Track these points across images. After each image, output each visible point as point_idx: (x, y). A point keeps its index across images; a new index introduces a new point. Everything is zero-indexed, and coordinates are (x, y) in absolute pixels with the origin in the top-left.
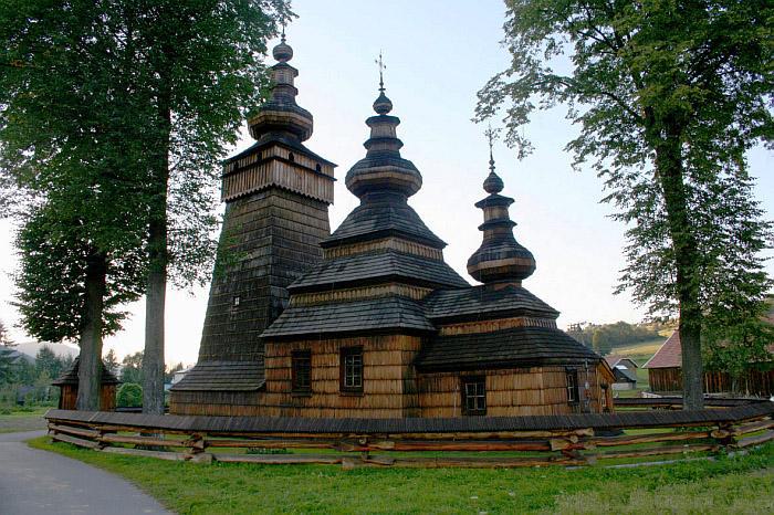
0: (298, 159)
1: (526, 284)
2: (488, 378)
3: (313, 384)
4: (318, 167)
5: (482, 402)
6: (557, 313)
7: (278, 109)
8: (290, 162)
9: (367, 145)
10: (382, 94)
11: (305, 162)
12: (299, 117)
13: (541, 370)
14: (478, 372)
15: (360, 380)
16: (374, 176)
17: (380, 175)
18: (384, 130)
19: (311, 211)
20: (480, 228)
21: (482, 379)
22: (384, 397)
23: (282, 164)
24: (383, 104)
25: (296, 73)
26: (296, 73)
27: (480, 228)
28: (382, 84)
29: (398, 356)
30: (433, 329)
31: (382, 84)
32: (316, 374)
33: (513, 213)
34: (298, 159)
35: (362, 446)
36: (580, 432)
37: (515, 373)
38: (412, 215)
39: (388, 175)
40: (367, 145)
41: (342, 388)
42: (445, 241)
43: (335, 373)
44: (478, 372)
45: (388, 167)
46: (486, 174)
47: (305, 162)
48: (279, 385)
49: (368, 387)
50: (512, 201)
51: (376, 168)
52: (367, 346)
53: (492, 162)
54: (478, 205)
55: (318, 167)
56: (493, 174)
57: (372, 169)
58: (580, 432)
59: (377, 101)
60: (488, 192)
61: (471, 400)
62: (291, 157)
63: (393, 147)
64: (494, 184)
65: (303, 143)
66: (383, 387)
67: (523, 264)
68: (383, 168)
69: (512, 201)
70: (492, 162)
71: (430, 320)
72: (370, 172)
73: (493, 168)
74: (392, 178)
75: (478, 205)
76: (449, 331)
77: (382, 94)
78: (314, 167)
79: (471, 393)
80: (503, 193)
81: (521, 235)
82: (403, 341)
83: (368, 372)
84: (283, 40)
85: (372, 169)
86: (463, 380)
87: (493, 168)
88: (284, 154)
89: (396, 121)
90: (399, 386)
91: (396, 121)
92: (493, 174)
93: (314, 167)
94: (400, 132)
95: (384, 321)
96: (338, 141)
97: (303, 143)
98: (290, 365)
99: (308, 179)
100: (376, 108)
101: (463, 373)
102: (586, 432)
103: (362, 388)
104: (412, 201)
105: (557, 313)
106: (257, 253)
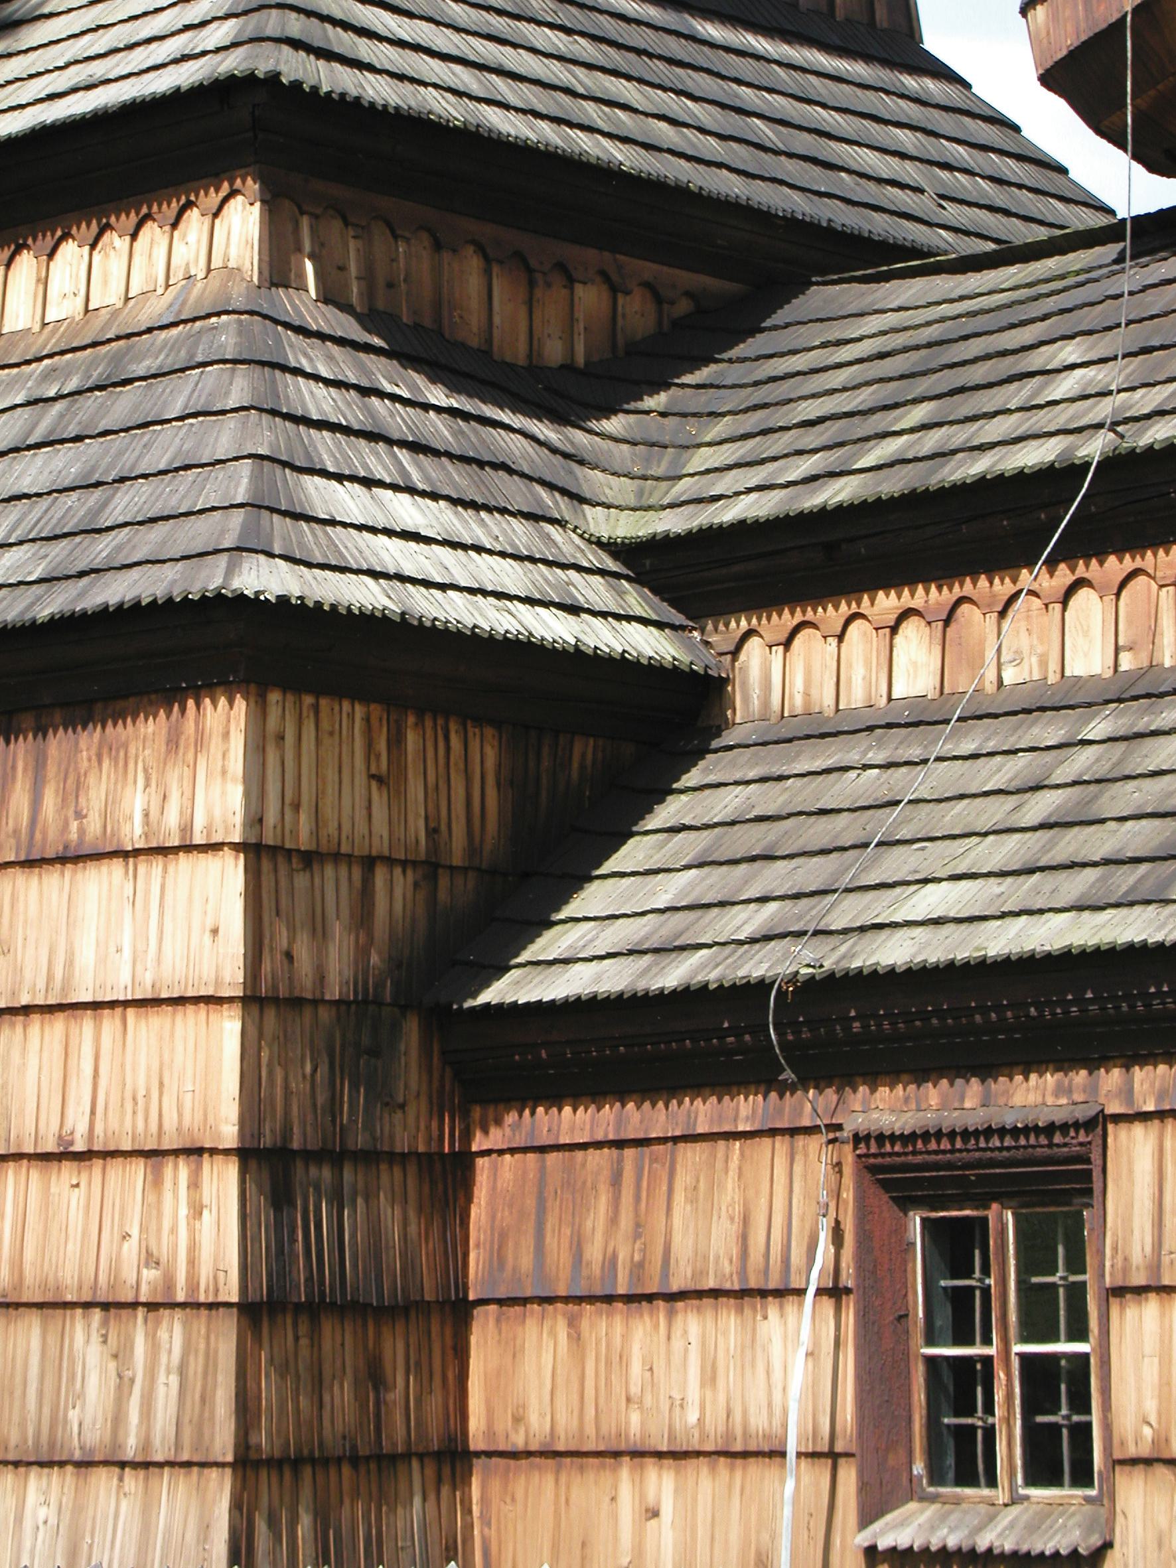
2: (1133, 1156)
5: (1061, 1391)
14: (1034, 1095)
21: (1057, 1182)
22: (85, 1338)
29: (201, 920)
30: (648, 644)
61: (962, 1385)
71: (642, 561)
76: (787, 667)
79: (961, 1315)
82: (199, 769)
86: (896, 1173)
90: (205, 1229)
95: (101, 549)
101: (886, 1108)
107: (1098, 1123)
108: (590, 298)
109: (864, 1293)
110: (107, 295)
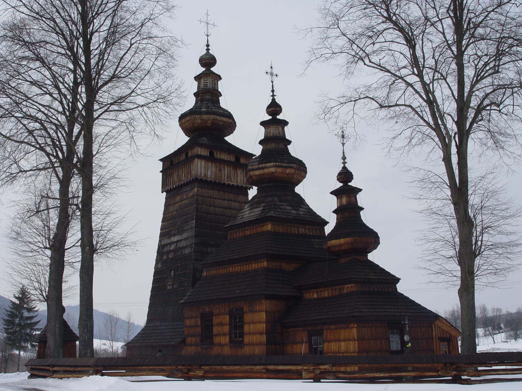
0: (219, 155)
1: (372, 256)
2: (325, 332)
3: (214, 338)
4: (237, 159)
6: (397, 280)
7: (201, 113)
8: (210, 158)
9: (261, 143)
10: (274, 100)
11: (224, 157)
12: (218, 118)
13: (355, 326)
14: (319, 328)
15: (242, 335)
16: (262, 172)
17: (266, 171)
18: (274, 130)
19: (232, 196)
20: (334, 212)
24: (274, 108)
25: (219, 78)
26: (219, 78)
27: (334, 212)
28: (273, 91)
31: (273, 91)
32: (215, 330)
33: (361, 199)
34: (219, 155)
35: (186, 373)
37: (340, 329)
38: (300, 201)
39: (273, 170)
40: (261, 143)
41: (231, 341)
42: (327, 220)
43: (226, 329)
44: (319, 328)
45: (272, 164)
46: (339, 168)
47: (224, 157)
48: (193, 339)
49: (247, 339)
50: (360, 190)
51: (263, 165)
52: (245, 309)
53: (344, 158)
54: (332, 193)
55: (237, 159)
56: (344, 168)
57: (260, 166)
58: (322, 367)
59: (268, 108)
62: (211, 154)
63: (281, 146)
64: (345, 176)
65: (227, 139)
66: (255, 338)
67: (372, 239)
68: (268, 165)
69: (360, 190)
70: (344, 158)
72: (258, 169)
73: (344, 163)
74: (276, 172)
75: (332, 193)
77: (274, 100)
78: (232, 159)
80: (352, 184)
81: (367, 218)
83: (246, 328)
84: (208, 50)
85: (260, 166)
87: (344, 163)
89: (285, 123)
90: (263, 338)
91: (285, 123)
92: (344, 168)
93: (232, 159)
94: (289, 132)
96: (247, 138)
97: (227, 139)
98: (199, 324)
99: (226, 170)
100: (269, 113)
101: (310, 328)
102: (326, 367)
103: (243, 340)
104: (298, 189)
105: (397, 280)
106: (185, 235)
107: (323, 330)
108: (294, 265)
109: (310, 342)
110: (256, 267)
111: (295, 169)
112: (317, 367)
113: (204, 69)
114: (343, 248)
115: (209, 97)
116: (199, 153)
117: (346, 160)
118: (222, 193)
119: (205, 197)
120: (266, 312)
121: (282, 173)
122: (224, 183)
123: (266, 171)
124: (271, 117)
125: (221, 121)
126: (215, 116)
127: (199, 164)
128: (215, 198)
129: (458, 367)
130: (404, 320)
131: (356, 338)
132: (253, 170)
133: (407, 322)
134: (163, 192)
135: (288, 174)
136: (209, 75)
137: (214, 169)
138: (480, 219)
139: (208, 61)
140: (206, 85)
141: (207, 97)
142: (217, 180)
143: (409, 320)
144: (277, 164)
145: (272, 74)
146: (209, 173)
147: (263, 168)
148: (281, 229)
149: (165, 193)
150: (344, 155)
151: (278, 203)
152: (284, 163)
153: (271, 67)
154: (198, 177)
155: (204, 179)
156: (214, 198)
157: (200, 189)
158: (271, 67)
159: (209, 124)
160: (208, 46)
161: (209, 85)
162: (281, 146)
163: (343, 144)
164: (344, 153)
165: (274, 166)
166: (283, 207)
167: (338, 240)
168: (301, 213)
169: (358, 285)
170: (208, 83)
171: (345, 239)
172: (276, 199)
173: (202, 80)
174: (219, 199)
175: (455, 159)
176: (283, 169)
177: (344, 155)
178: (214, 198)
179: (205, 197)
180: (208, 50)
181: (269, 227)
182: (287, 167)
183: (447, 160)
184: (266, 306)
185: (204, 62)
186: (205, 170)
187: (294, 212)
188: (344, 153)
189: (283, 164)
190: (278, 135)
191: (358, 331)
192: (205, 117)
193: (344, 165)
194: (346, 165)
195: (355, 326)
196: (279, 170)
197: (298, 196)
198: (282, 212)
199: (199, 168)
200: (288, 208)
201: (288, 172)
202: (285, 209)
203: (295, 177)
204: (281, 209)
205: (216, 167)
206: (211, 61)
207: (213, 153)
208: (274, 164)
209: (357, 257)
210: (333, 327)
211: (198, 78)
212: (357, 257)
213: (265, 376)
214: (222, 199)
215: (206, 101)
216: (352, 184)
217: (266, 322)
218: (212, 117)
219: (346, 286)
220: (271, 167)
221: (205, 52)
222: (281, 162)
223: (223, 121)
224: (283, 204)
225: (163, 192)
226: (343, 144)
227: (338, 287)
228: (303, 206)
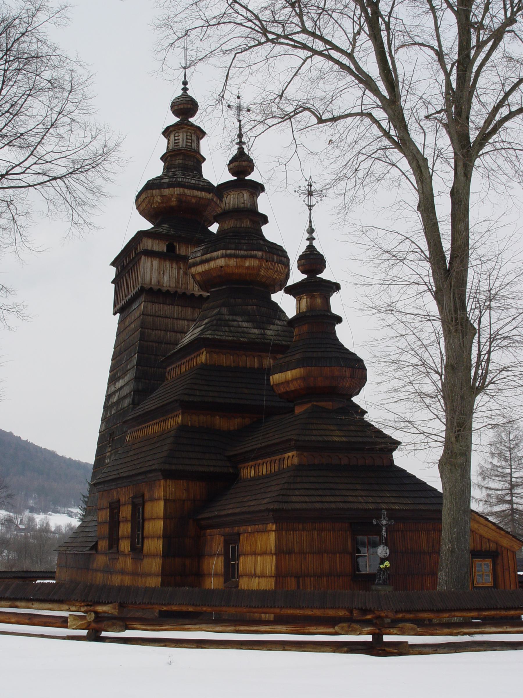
10: (241, 151)
12: (188, 192)
23: (156, 263)
36: (100, 609)
39: (221, 262)
44: (236, 529)
45: (220, 253)
51: (208, 256)
53: (311, 231)
56: (311, 248)
57: (204, 257)
58: (100, 609)
59: (231, 162)
60: (303, 272)
62: (171, 248)
63: (247, 223)
68: (215, 254)
70: (311, 231)
73: (311, 239)
74: (228, 266)
77: (241, 151)
84: (185, 89)
85: (204, 257)
87: (311, 239)
88: (160, 246)
92: (311, 248)
107: (239, 534)
111: (260, 259)
112: (92, 608)
113: (179, 119)
114: (292, 387)
115: (181, 161)
116: (149, 248)
117: (313, 235)
118: (189, 309)
119: (158, 316)
120: (166, 501)
121: (237, 267)
122: (193, 295)
123: (212, 264)
124: (235, 178)
125: (193, 196)
126: (182, 190)
127: (149, 264)
128: (177, 319)
129: (379, 617)
130: (379, 518)
131: (273, 551)
132: (195, 265)
133: (384, 522)
134: (115, 314)
135: (248, 268)
136: (182, 128)
137: (175, 272)
138: (487, 321)
139: (182, 107)
140: (176, 144)
141: (177, 162)
142: (179, 290)
143: (390, 518)
144: (229, 252)
145: (239, 108)
146: (166, 278)
147: (207, 261)
148: (225, 360)
149: (118, 315)
150: (311, 226)
151: (227, 317)
152: (241, 250)
153: (238, 97)
154: (145, 286)
155: (156, 288)
156: (173, 318)
157: (150, 304)
158: (238, 97)
159: (174, 202)
160: (185, 83)
161: (181, 143)
162: (247, 223)
163: (310, 207)
164: (310, 222)
165: (222, 256)
166: (235, 324)
167: (283, 374)
168: (268, 332)
169: (305, 454)
170: (180, 141)
171: (294, 371)
172: (224, 310)
173: (172, 136)
174: (184, 319)
175: (443, 207)
176: (239, 260)
177: (311, 226)
178: (173, 318)
179: (158, 316)
180: (185, 89)
181: (203, 358)
182: (245, 257)
183: (427, 207)
184: (165, 490)
185: (176, 108)
186: (159, 273)
187: (256, 331)
188: (310, 222)
189: (239, 252)
190: (242, 205)
191: (278, 539)
192: (167, 192)
193: (311, 243)
194: (314, 243)
195: (274, 527)
196: (233, 262)
197: (275, 304)
198: (230, 332)
199: (148, 270)
200: (245, 324)
201: (247, 264)
202: (240, 327)
203: (262, 272)
204: (229, 326)
205: (179, 269)
206: (186, 106)
207: (175, 247)
208: (224, 251)
209: (319, 404)
210: (250, 529)
211: (167, 132)
212: (319, 404)
213: (13, 620)
214: (188, 320)
215: (174, 168)
216: (324, 275)
217: (165, 518)
218: (177, 191)
219: (286, 455)
220: (218, 258)
221: (180, 93)
222: (236, 249)
223: (196, 197)
224: (238, 318)
225: (115, 314)
226: (310, 207)
227: (278, 457)
228: (277, 322)
